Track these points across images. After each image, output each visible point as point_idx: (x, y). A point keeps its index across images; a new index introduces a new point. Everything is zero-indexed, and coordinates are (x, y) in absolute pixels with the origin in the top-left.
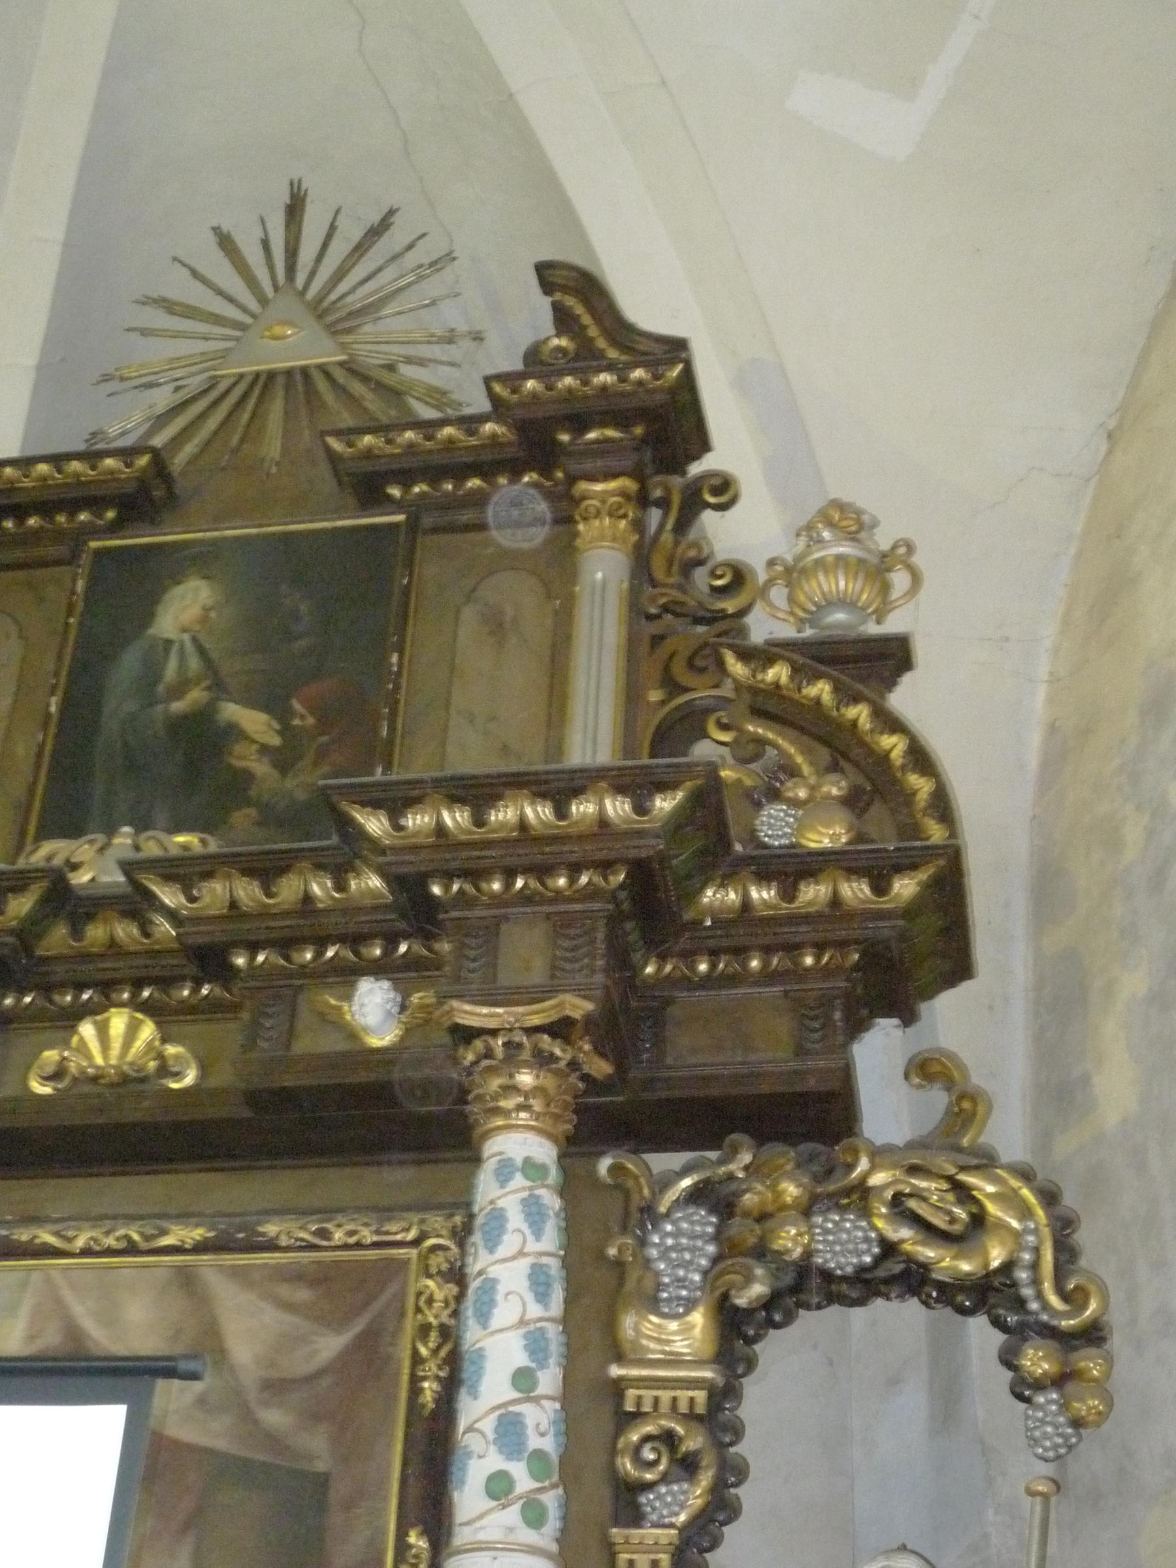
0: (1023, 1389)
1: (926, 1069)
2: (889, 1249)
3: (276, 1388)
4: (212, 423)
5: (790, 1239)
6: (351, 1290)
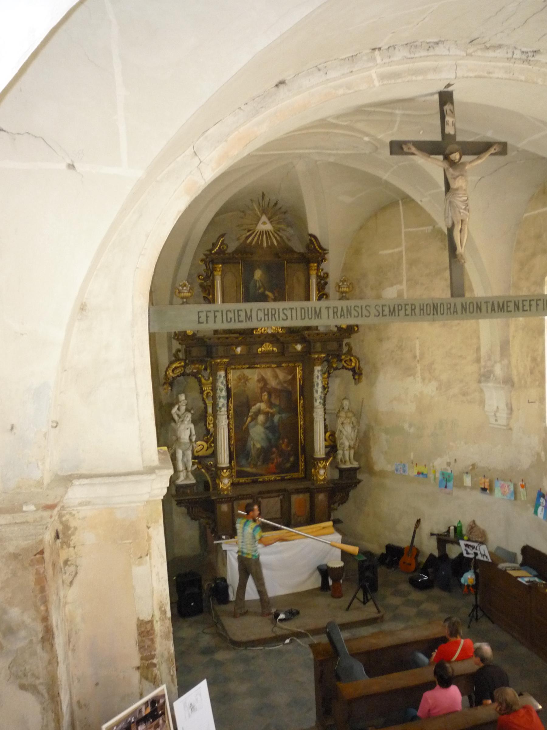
0: (354, 379)
1: (348, 344)
3: (285, 382)
4: (256, 239)
5: (334, 366)
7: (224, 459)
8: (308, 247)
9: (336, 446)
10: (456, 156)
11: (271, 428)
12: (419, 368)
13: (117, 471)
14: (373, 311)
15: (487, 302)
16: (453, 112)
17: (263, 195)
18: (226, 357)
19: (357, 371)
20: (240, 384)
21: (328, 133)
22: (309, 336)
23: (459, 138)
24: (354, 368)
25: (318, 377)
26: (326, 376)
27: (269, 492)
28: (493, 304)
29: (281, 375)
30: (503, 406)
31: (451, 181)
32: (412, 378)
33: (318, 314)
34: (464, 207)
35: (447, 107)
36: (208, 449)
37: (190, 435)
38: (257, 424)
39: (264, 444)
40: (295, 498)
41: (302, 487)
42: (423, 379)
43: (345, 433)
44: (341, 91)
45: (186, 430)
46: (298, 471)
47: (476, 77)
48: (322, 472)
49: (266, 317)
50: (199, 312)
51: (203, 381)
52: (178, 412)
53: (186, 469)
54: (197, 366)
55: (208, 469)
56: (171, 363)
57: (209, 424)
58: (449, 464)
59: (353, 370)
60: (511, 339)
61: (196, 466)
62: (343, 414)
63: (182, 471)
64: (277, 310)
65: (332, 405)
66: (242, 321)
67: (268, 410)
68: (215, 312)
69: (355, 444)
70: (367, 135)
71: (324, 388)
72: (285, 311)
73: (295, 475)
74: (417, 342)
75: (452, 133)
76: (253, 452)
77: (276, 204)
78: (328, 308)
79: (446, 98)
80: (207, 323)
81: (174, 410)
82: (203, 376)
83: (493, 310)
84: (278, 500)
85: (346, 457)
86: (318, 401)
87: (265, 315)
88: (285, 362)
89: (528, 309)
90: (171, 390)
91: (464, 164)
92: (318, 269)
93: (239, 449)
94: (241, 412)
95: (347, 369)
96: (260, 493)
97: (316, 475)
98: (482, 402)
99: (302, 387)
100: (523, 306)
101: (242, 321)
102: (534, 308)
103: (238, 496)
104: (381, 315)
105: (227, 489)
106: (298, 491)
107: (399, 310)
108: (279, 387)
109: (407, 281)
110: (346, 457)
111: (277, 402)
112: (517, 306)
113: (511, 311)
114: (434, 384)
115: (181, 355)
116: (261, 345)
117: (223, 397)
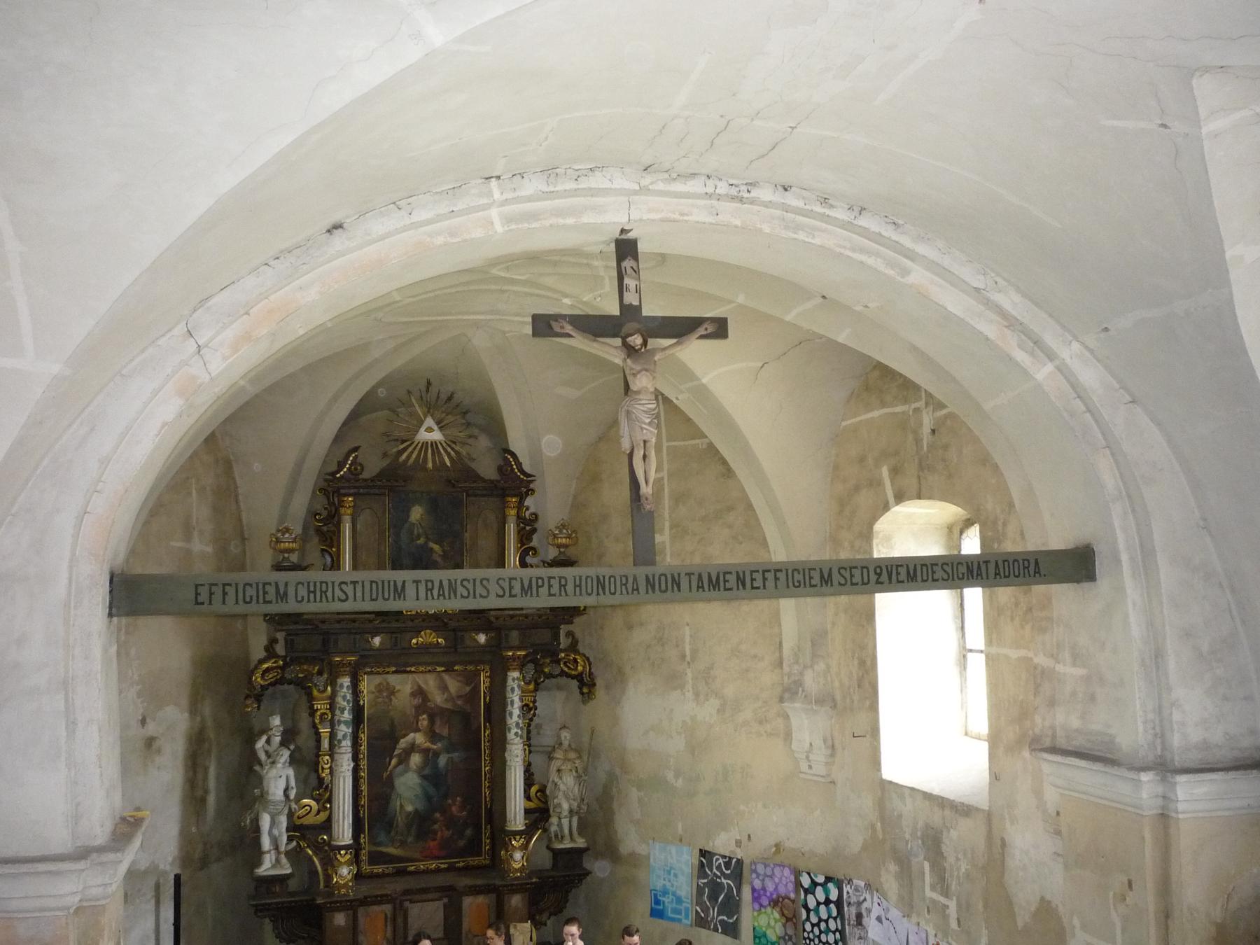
0: (582, 694)
1: (570, 634)
2: (562, 670)
3: (459, 697)
4: (414, 456)
6: (471, 679)
7: (344, 832)
8: (500, 469)
9: (547, 810)
10: (636, 340)
11: (432, 777)
12: (690, 675)
13: (23, 854)
14: (494, 588)
15: (689, 574)
16: (636, 271)
17: (429, 383)
18: (351, 653)
19: (586, 679)
21: (503, 291)
22: (497, 618)
23: (645, 313)
24: (581, 674)
25: (513, 690)
26: (531, 687)
27: (425, 891)
28: (700, 576)
29: (453, 685)
30: (818, 743)
31: (630, 379)
32: (679, 691)
33: (400, 592)
34: (648, 421)
35: (628, 264)
36: (318, 812)
37: (286, 790)
38: (407, 770)
39: (420, 806)
40: (468, 902)
41: (479, 882)
42: (697, 695)
43: (562, 787)
44: (440, 240)
45: (279, 779)
46: (479, 854)
47: (662, 220)
48: (518, 855)
49: (312, 595)
50: (197, 586)
51: (315, 693)
53: (277, 848)
54: (305, 667)
55: (318, 848)
56: (261, 662)
58: (738, 843)
59: (579, 677)
60: (829, 626)
61: (294, 843)
62: (559, 754)
63: (269, 852)
64: (330, 585)
65: (546, 738)
66: (270, 602)
67: (428, 744)
68: (224, 585)
69: (579, 806)
70: (567, 296)
71: (528, 709)
72: (343, 586)
73: (473, 861)
74: (687, 630)
75: (636, 303)
76: (400, 820)
77: (450, 398)
78: (417, 582)
79: (626, 248)
80: (210, 603)
81: (260, 744)
82: (316, 685)
83: (700, 587)
84: (439, 905)
85: (565, 828)
86: (514, 730)
87: (309, 592)
88: (460, 663)
89: (761, 585)
90: (259, 708)
91: (653, 352)
92: (520, 505)
93: (374, 810)
94: (379, 747)
95: (568, 676)
96: (407, 892)
97: (509, 864)
98: (788, 736)
99: (488, 708)
100: (752, 580)
101: (270, 602)
102: (770, 583)
103: (366, 898)
104: (507, 594)
105: (346, 885)
106: (475, 891)
107: (538, 587)
108: (449, 706)
109: (671, 528)
110: (565, 828)
111: (445, 732)
112: (741, 581)
113: (730, 589)
114: (714, 703)
115: (280, 649)
116: (417, 633)
117: (346, 723)
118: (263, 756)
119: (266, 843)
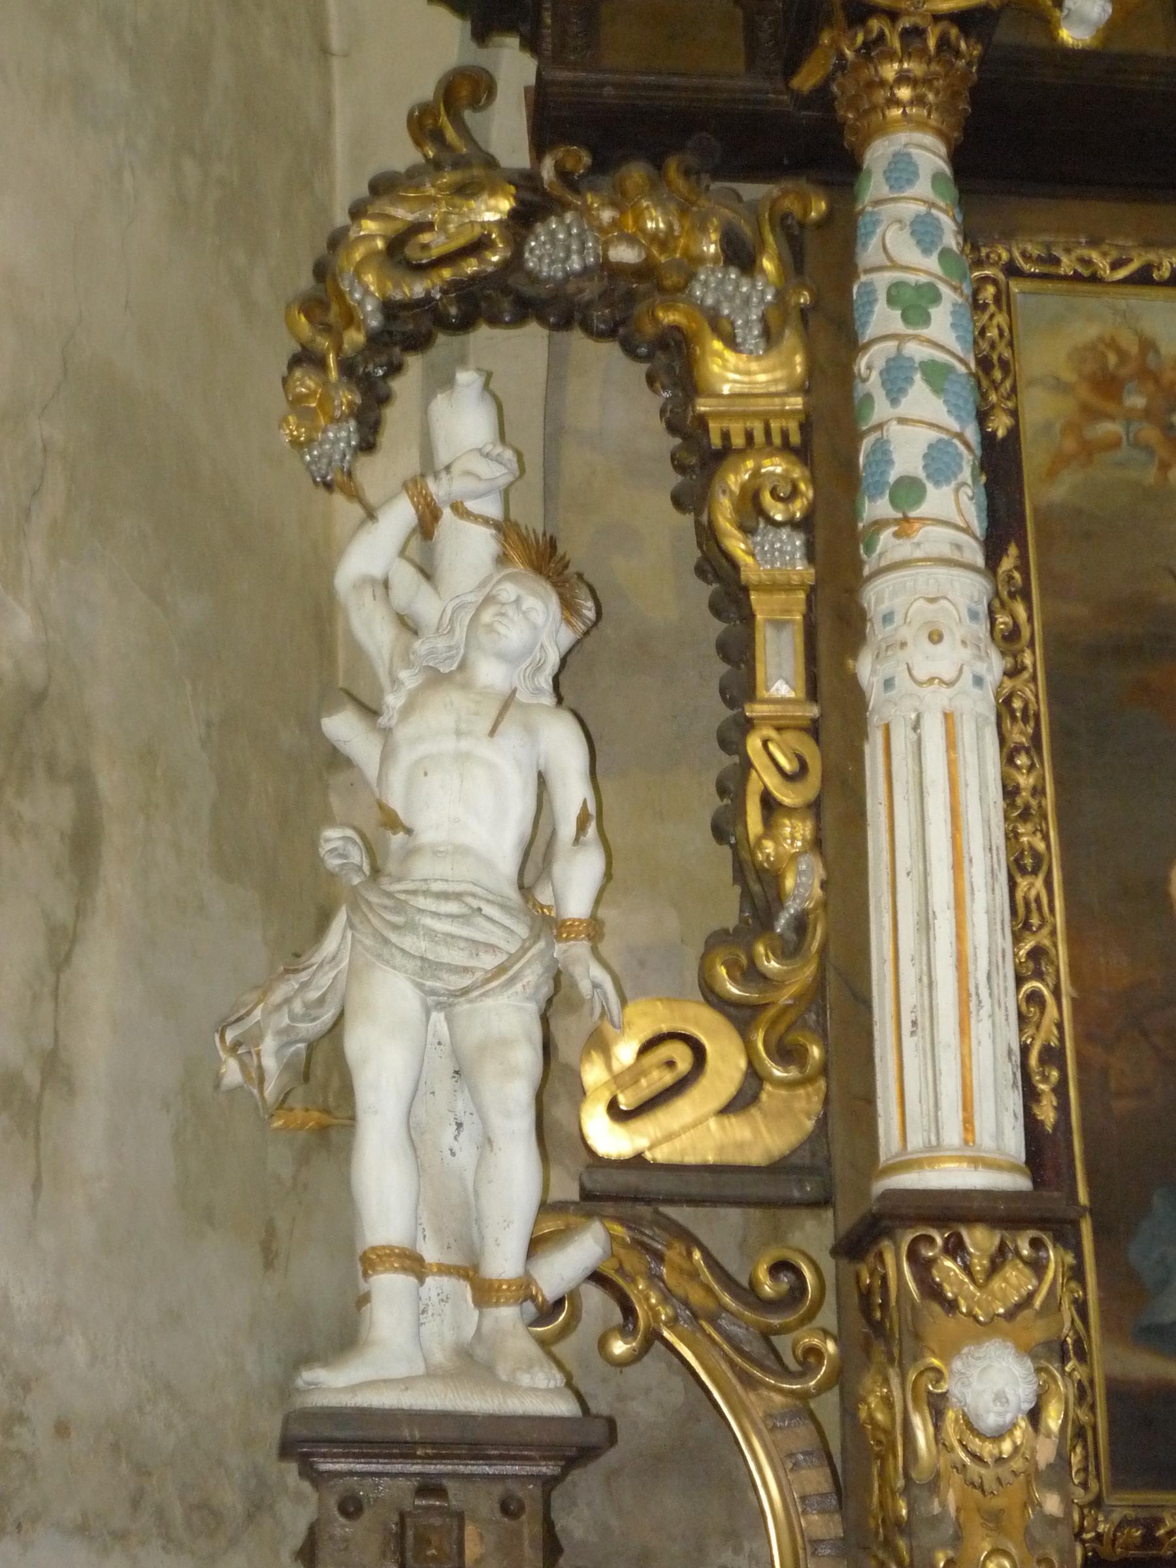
20: (1109, 428)
37: (537, 856)
52: (405, 577)
57: (769, 804)
118: (372, 629)
119: (386, 1194)
